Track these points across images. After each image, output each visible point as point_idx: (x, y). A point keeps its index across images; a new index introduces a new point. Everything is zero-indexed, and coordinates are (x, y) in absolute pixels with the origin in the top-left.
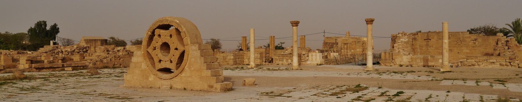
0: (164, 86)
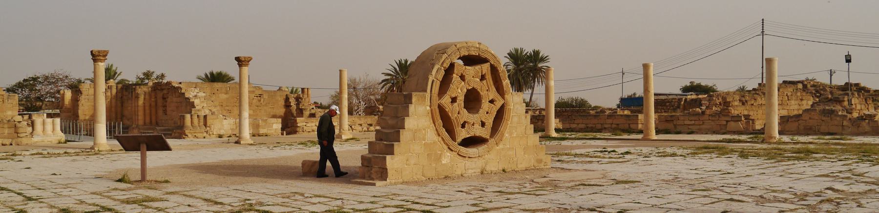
0: (470, 171)
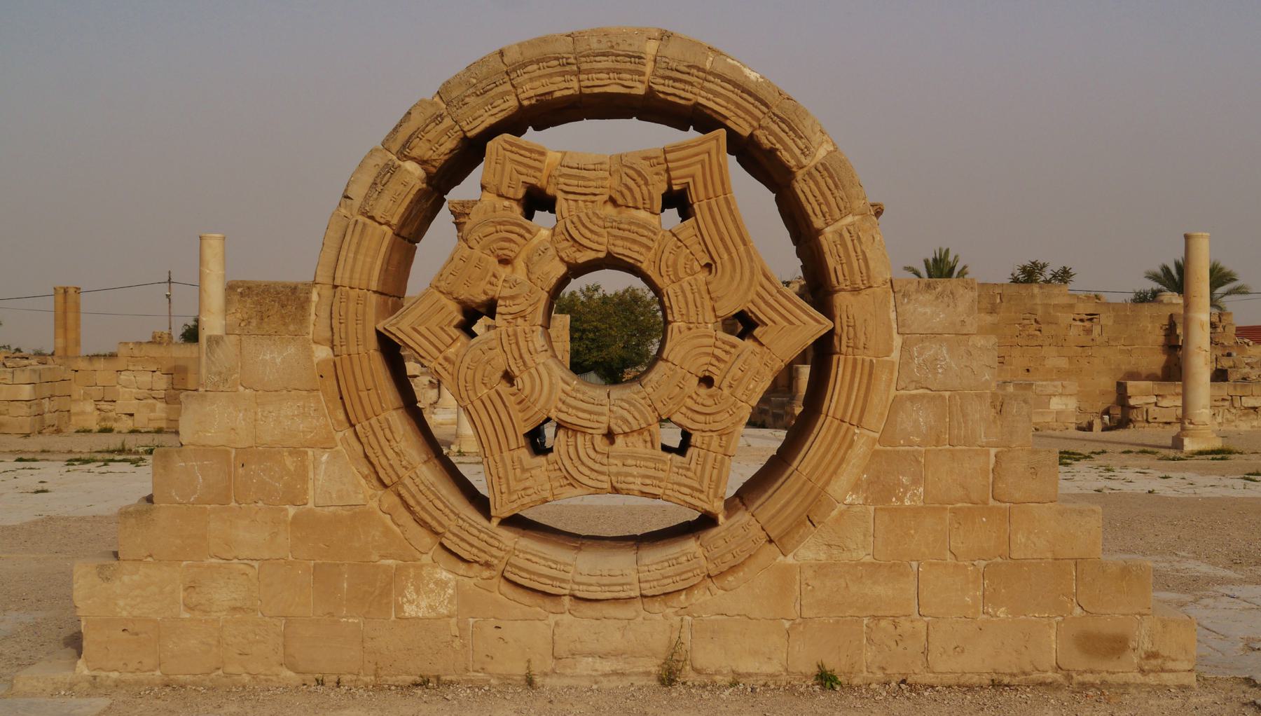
0: (586, 665)
